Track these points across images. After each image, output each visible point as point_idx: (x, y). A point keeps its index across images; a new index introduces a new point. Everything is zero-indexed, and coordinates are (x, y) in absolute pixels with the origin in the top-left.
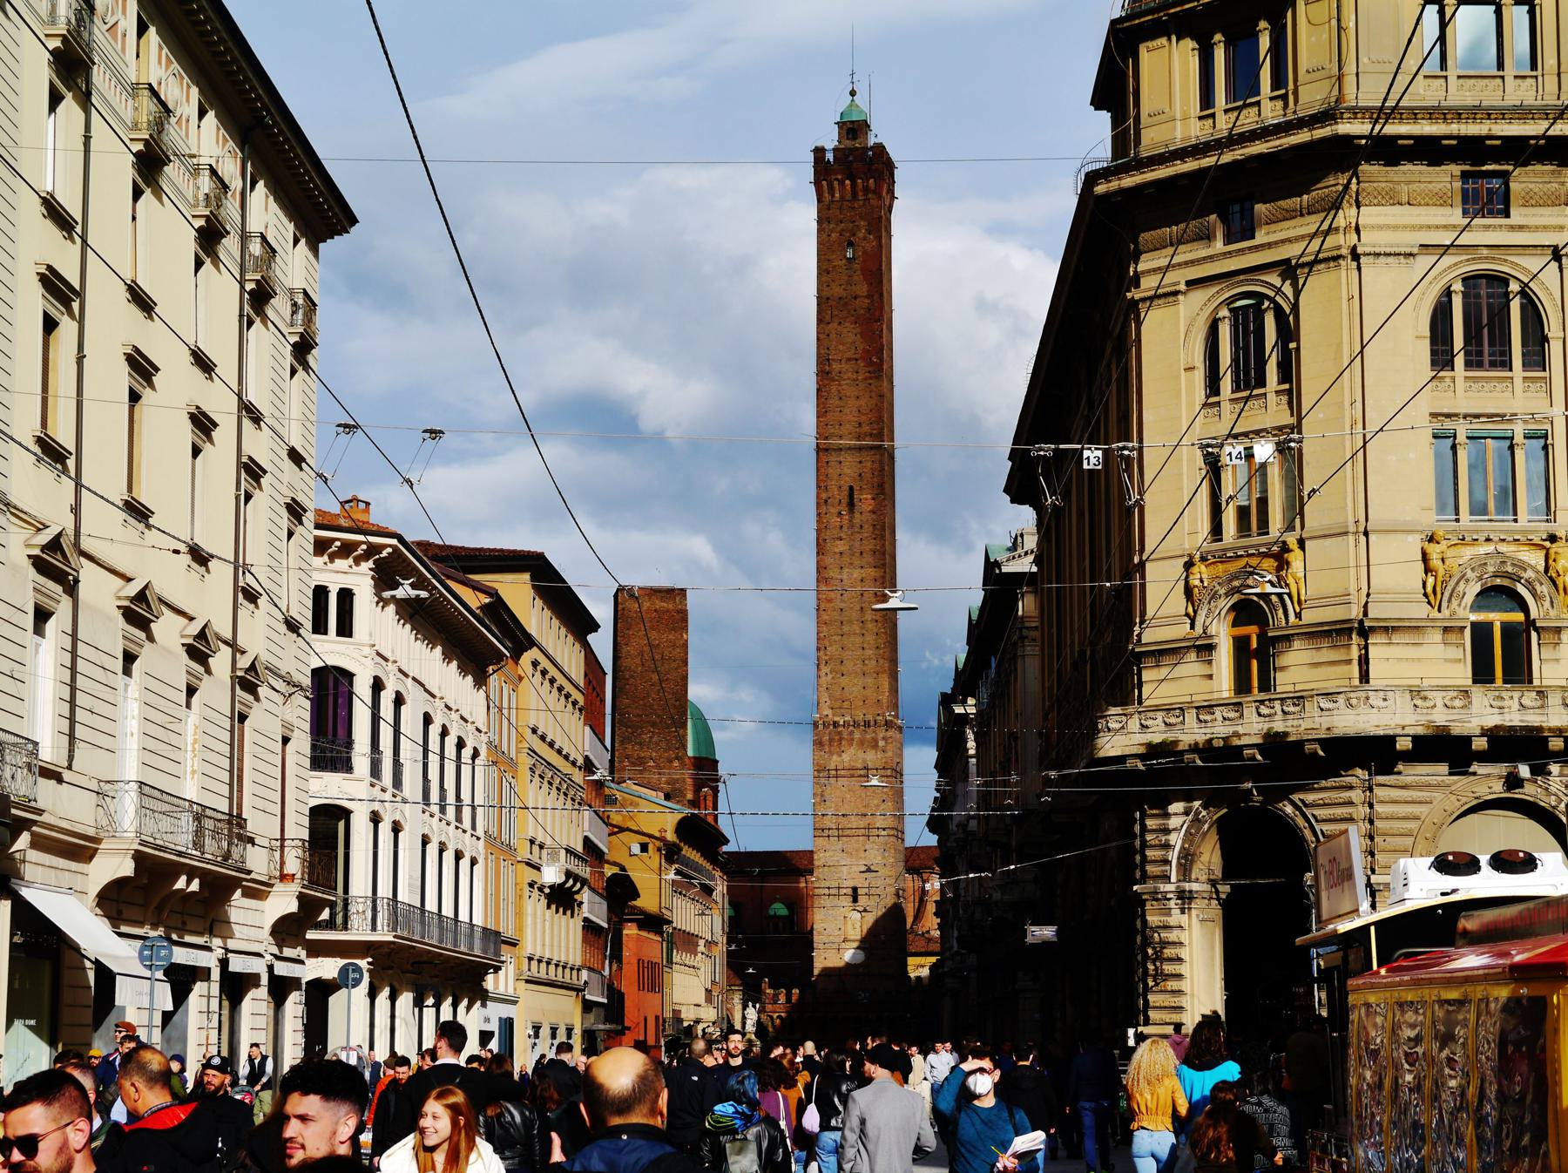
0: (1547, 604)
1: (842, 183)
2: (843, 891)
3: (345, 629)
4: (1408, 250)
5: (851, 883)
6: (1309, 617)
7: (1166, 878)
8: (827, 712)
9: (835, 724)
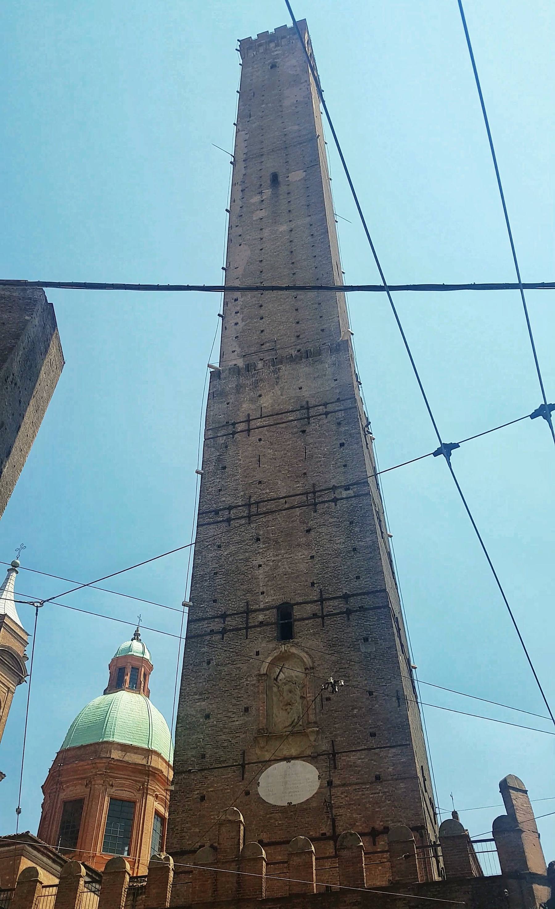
2: (261, 617)
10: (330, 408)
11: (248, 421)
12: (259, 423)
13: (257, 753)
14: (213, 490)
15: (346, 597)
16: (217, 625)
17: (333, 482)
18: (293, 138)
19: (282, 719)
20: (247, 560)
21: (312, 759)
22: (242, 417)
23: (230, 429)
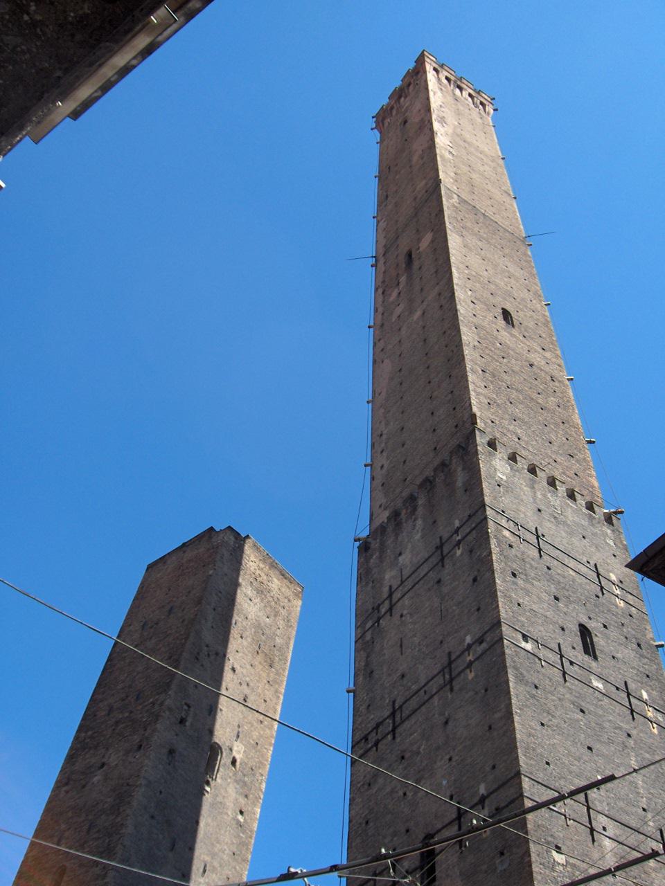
14: (363, 708)
18: (421, 198)
20: (393, 791)
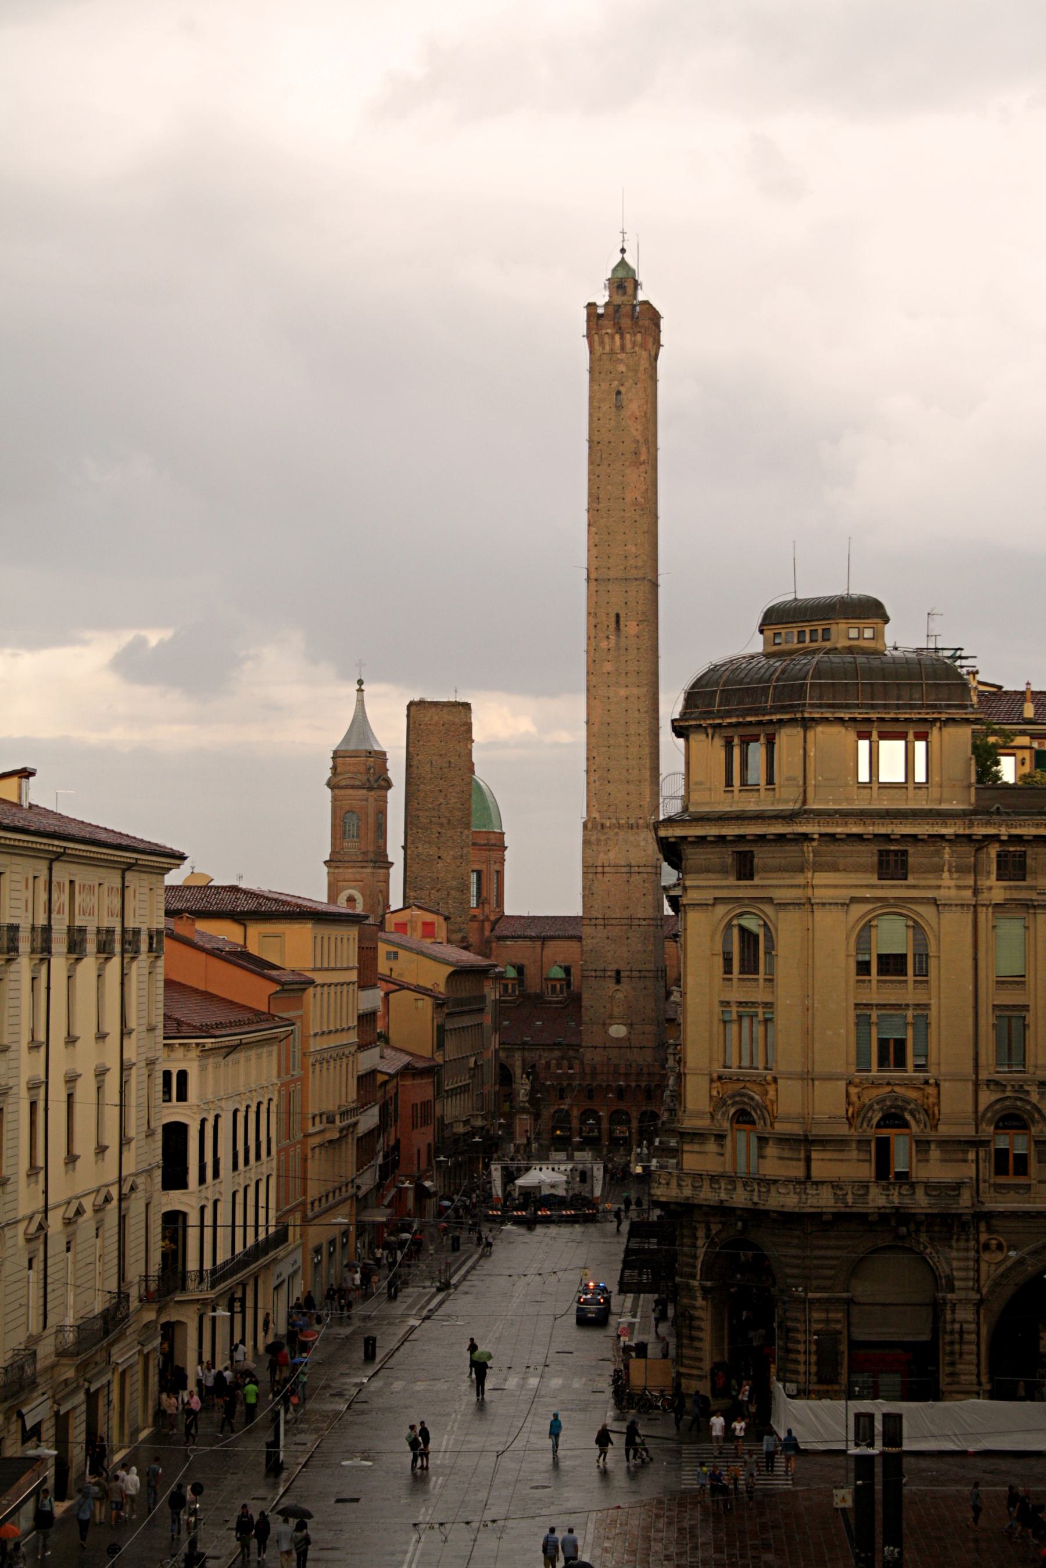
0: (922, 1126)
1: (613, 338)
2: (609, 973)
3: (182, 1097)
4: (842, 901)
5: (614, 967)
6: (779, 1127)
7: (693, 1276)
8: (596, 815)
9: (603, 826)
10: (641, 870)
11: (603, 867)
12: (607, 869)
13: (608, 1021)
15: (640, 971)
16: (593, 974)
17: (639, 916)
19: (616, 1011)
21: (625, 1025)
22: (599, 863)
23: (593, 870)
